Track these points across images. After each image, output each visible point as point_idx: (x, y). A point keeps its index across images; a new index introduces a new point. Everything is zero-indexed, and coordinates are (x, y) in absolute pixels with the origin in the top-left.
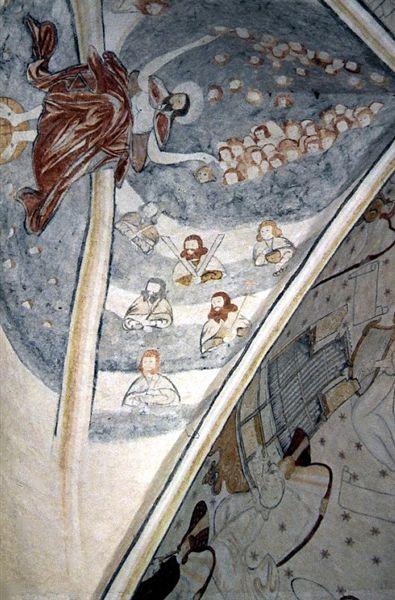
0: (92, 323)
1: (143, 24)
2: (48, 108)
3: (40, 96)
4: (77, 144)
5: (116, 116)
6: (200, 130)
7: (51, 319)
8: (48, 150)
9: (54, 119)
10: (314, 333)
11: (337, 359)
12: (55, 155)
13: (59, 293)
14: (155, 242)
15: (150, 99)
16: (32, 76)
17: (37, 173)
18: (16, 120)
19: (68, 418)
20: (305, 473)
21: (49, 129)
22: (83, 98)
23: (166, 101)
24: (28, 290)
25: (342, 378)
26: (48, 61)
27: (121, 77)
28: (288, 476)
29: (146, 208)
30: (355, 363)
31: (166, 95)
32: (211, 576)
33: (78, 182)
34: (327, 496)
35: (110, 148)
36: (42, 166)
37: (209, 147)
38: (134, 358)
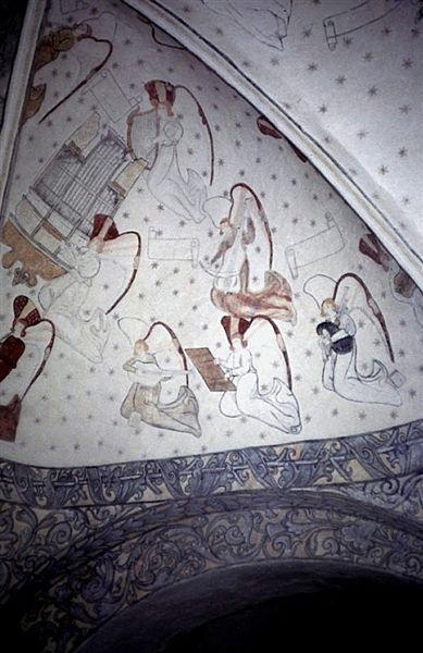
20: (113, 244)
25: (125, 164)
28: (100, 251)
32: (54, 335)
34: (139, 254)
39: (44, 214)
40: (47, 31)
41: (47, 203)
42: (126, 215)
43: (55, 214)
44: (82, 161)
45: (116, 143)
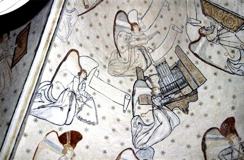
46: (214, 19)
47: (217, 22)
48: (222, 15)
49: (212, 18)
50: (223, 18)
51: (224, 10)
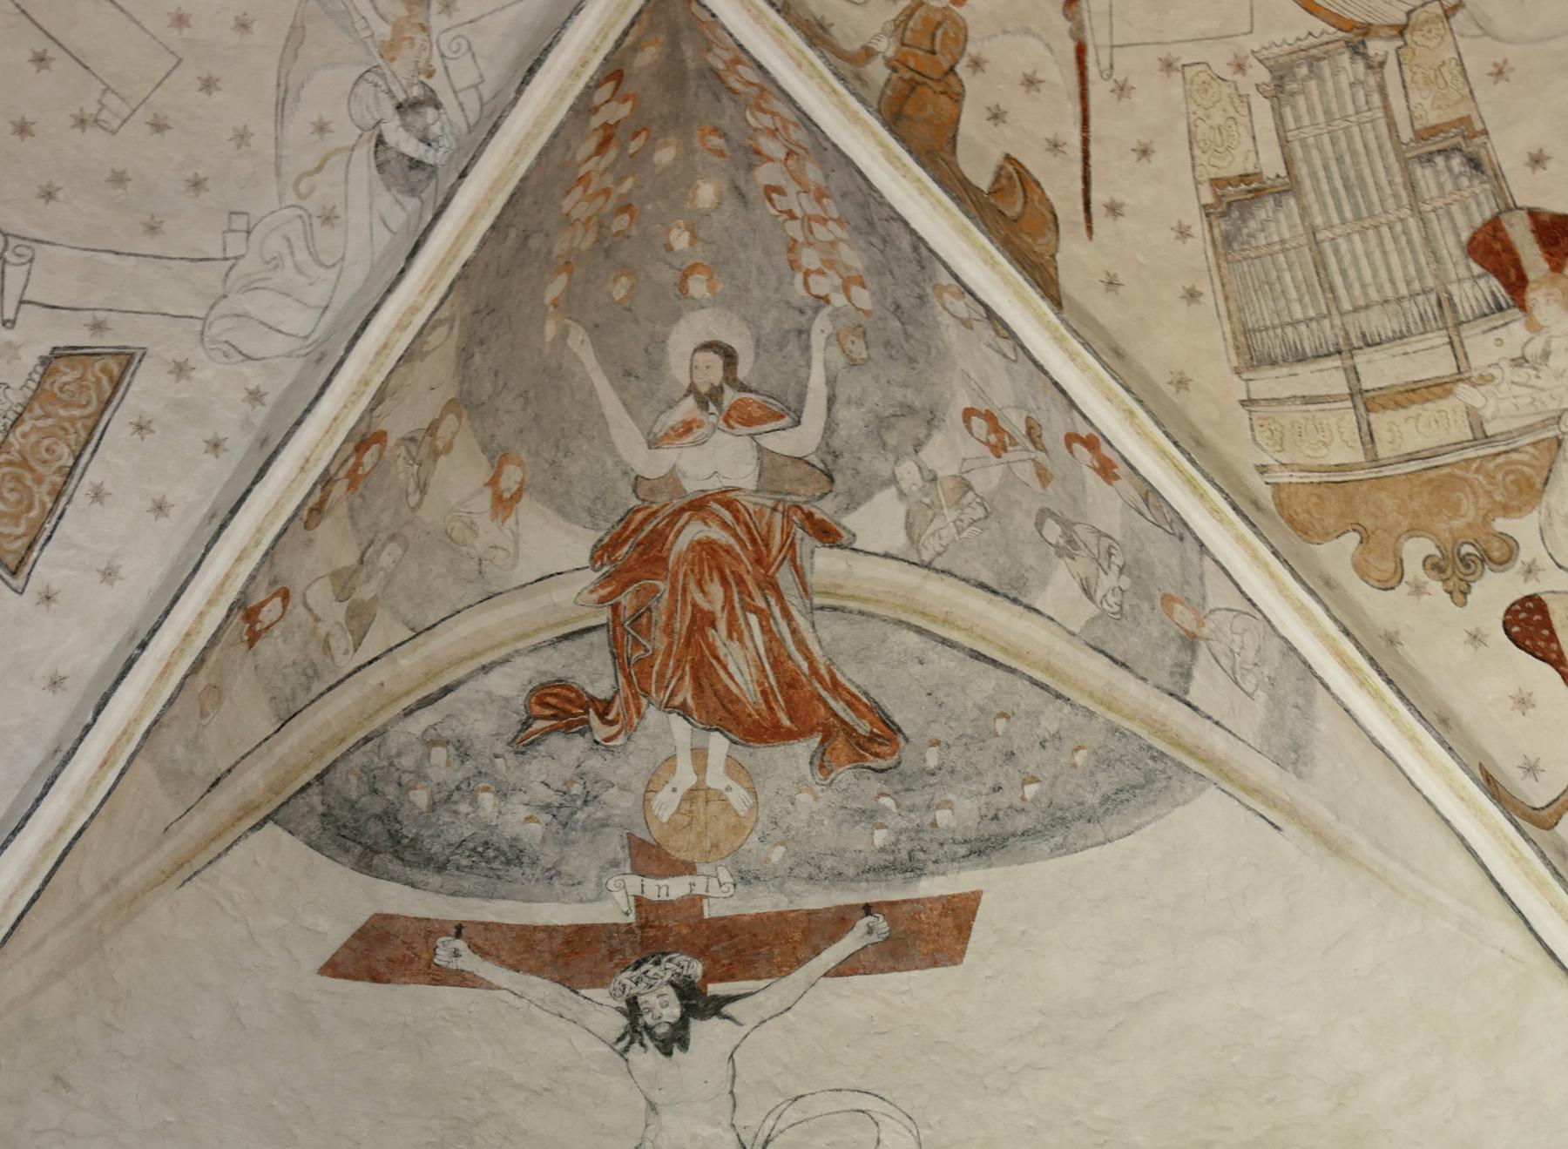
0: (1098, 667)
1: (543, 492)
2: (677, 701)
3: (653, 715)
4: (752, 637)
5: (717, 534)
6: (768, 323)
7: (1069, 744)
8: (750, 709)
9: (699, 689)
10: (1228, 182)
11: (1330, 87)
12: (763, 693)
13: (1028, 714)
14: (969, 488)
15: (695, 444)
16: (619, 733)
17: (789, 736)
18: (685, 776)
19: (1254, 791)
21: (713, 703)
22: (671, 615)
23: (703, 403)
24: (1004, 782)
25: (1391, 68)
26: (593, 699)
27: (645, 521)
29: (904, 485)
30: (1360, 17)
31: (690, 402)
33: (826, 638)
35: (774, 551)
36: (777, 725)
37: (802, 312)
38: (1173, 633)
39: (1337, 383)
40: (878, 72)
41: (1317, 357)
42: (1537, 161)
43: (1361, 359)
44: (1289, 187)
45: (1313, 61)
46: (27, 407)
47: (9, 423)
48: (44, 462)
49: (32, 398)
50: (33, 463)
51: (70, 474)
